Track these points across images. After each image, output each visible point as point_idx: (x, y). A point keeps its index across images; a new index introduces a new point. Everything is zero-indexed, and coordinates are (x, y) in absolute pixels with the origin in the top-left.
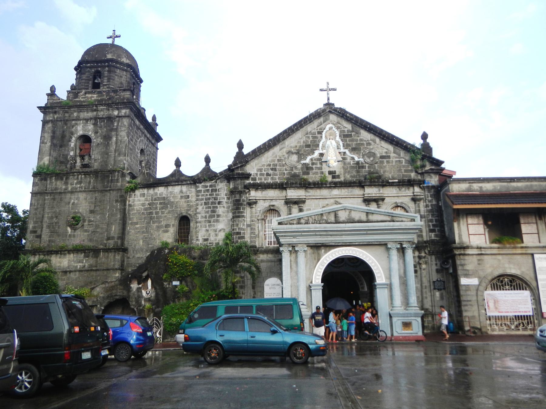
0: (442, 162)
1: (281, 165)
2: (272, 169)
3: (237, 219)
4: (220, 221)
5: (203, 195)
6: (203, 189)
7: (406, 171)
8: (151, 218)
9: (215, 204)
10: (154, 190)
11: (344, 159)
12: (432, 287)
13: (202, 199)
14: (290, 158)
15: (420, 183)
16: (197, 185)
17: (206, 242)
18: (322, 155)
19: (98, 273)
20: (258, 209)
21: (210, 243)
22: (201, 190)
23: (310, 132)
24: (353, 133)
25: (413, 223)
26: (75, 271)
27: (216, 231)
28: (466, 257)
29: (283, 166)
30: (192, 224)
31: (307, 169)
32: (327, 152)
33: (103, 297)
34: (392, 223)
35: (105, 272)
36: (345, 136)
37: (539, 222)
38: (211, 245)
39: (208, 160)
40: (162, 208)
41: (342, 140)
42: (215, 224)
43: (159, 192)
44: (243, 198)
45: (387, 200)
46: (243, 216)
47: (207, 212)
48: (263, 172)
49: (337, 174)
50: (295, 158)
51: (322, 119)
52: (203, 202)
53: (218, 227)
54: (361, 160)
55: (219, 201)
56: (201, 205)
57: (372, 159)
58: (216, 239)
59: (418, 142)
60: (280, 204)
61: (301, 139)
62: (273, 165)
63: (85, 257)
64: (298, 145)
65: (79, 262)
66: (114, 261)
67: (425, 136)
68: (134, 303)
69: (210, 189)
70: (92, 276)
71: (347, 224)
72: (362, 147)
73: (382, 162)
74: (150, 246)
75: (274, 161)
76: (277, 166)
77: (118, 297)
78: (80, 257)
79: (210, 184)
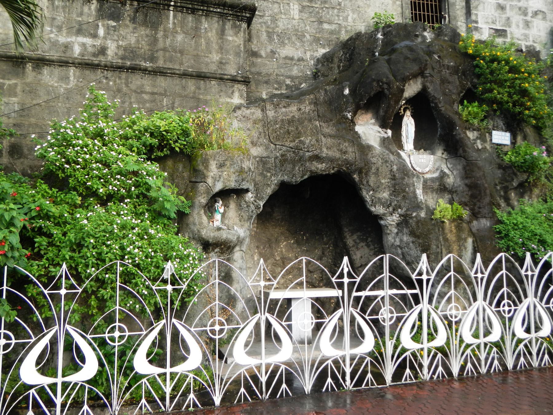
19: (162, 82)
26: (64, 63)
33: (262, 161)
35: (191, 85)
58: (526, 37)
63: (101, 14)
65: (79, 32)
66: (221, 48)
68: (385, 195)
70: (140, 91)
74: (326, 26)
77: (320, 167)
78: (81, 14)
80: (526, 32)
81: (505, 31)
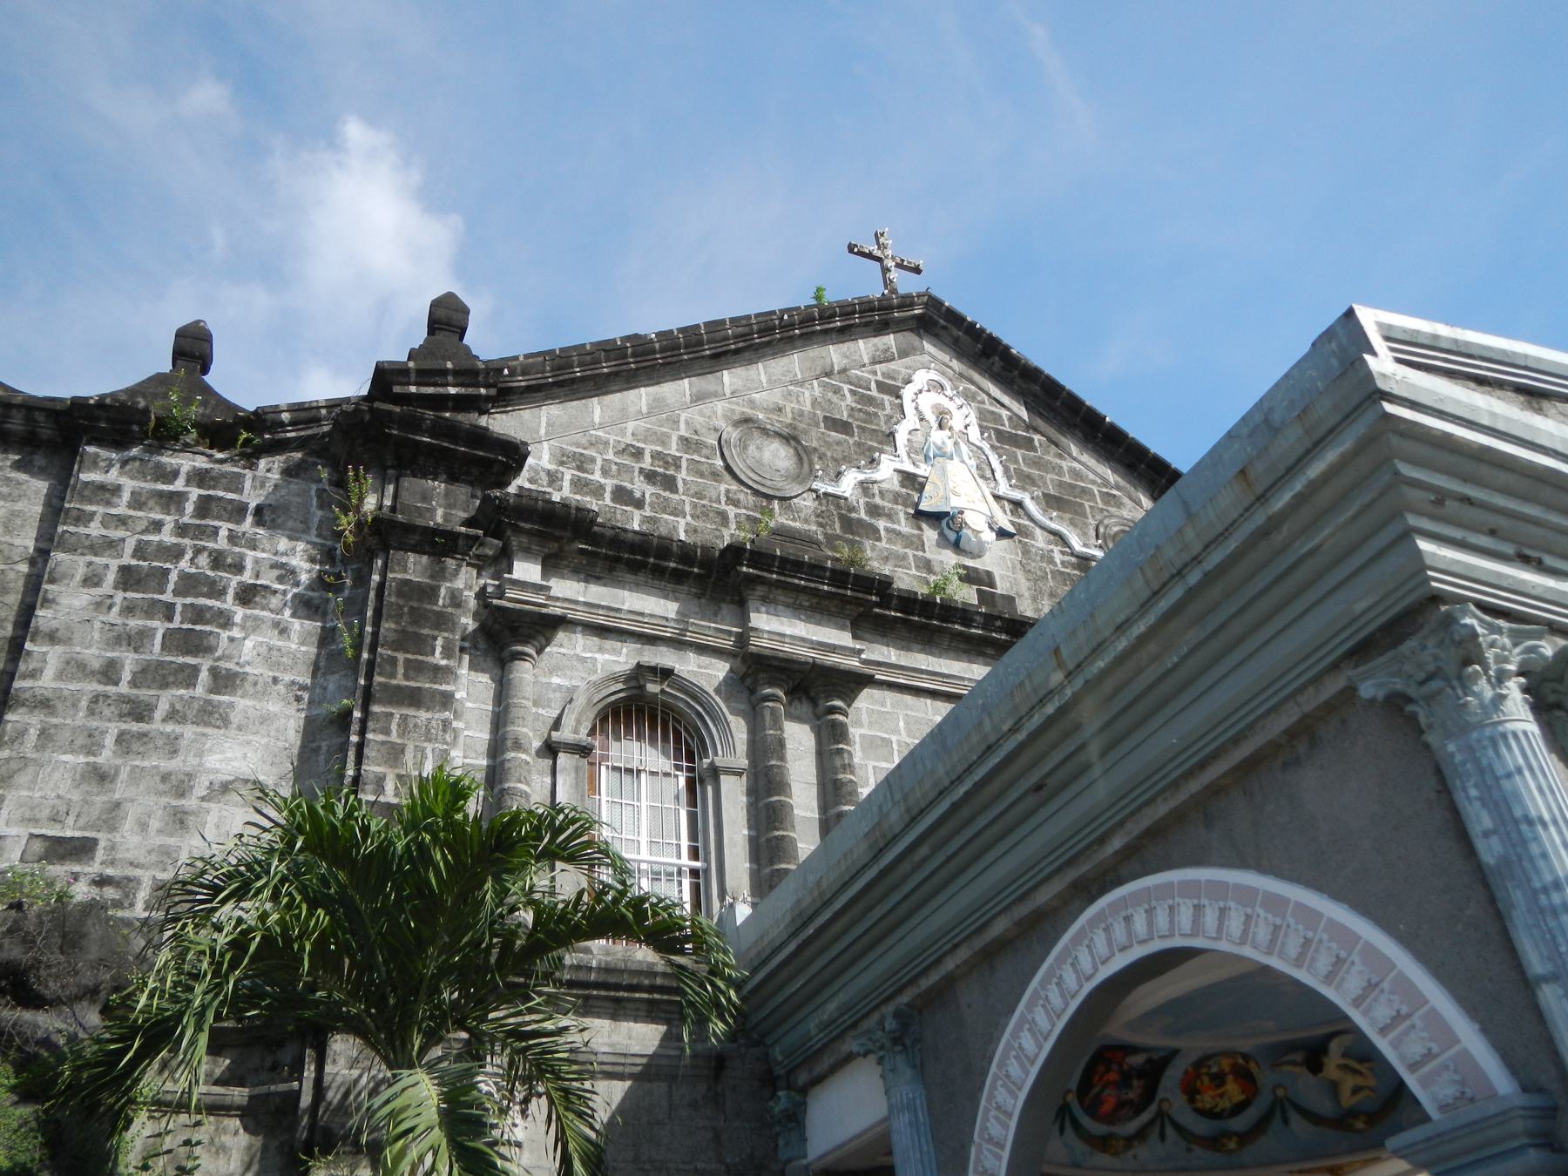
1: (704, 468)
2: (650, 477)
3: (397, 712)
4: (235, 717)
6: (129, 485)
9: (220, 593)
13: (111, 545)
14: (752, 448)
16: (91, 449)
17: (58, 870)
20: (556, 680)
21: (101, 881)
22: (116, 490)
23: (843, 371)
24: (1037, 437)
27: (182, 791)
29: (715, 476)
32: (944, 473)
38: (110, 893)
41: (993, 447)
42: (189, 731)
44: (459, 584)
46: (446, 700)
48: (597, 476)
50: (777, 456)
51: (890, 340)
52: (112, 565)
53: (212, 761)
55: (247, 577)
56: (92, 580)
61: (801, 383)
62: (656, 456)
64: (789, 407)
69: (195, 493)
72: (1087, 504)
75: (663, 440)
76: (678, 467)
79: (201, 462)
80: (172, 841)
81: (95, 841)
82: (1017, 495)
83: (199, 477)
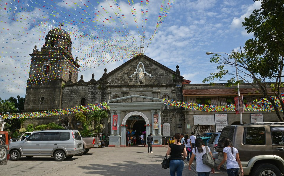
0: (183, 77)
2: (117, 80)
5: (90, 90)
7: (169, 81)
8: (71, 99)
10: (72, 87)
11: (145, 76)
12: (177, 127)
13: (90, 91)
15: (174, 86)
18: (137, 74)
23: (133, 65)
25: (160, 102)
28: (189, 115)
30: (86, 101)
31: (131, 80)
32: (139, 73)
34: (152, 103)
36: (146, 67)
37: (218, 101)
39: (93, 76)
40: (75, 95)
41: (145, 68)
43: (74, 88)
45: (161, 92)
46: (105, 98)
47: (92, 96)
49: (142, 82)
51: (138, 60)
52: (90, 92)
54: (152, 76)
56: (90, 93)
57: (156, 76)
59: (175, 70)
60: (119, 94)
67: (177, 67)
71: (135, 103)
73: (160, 77)
82: (145, 73)
83: (93, 86)
